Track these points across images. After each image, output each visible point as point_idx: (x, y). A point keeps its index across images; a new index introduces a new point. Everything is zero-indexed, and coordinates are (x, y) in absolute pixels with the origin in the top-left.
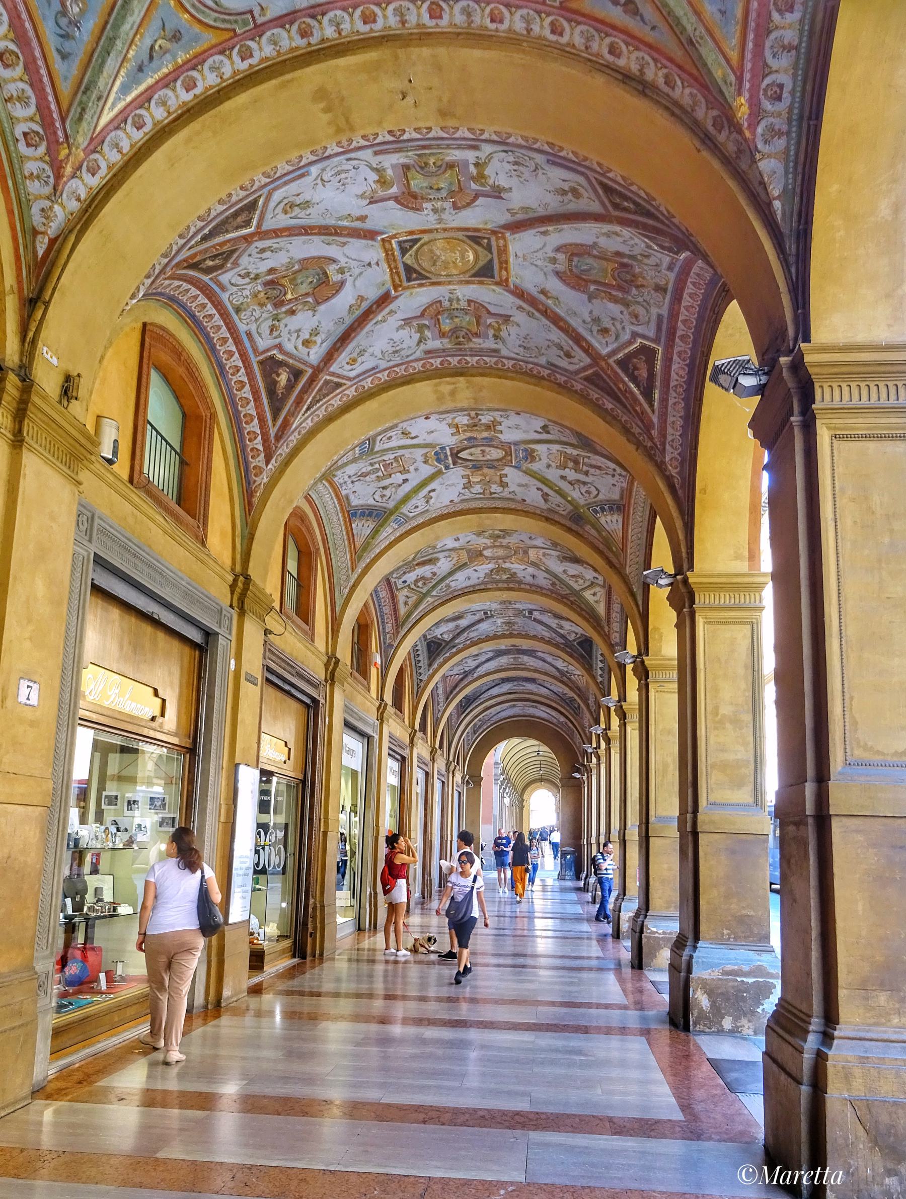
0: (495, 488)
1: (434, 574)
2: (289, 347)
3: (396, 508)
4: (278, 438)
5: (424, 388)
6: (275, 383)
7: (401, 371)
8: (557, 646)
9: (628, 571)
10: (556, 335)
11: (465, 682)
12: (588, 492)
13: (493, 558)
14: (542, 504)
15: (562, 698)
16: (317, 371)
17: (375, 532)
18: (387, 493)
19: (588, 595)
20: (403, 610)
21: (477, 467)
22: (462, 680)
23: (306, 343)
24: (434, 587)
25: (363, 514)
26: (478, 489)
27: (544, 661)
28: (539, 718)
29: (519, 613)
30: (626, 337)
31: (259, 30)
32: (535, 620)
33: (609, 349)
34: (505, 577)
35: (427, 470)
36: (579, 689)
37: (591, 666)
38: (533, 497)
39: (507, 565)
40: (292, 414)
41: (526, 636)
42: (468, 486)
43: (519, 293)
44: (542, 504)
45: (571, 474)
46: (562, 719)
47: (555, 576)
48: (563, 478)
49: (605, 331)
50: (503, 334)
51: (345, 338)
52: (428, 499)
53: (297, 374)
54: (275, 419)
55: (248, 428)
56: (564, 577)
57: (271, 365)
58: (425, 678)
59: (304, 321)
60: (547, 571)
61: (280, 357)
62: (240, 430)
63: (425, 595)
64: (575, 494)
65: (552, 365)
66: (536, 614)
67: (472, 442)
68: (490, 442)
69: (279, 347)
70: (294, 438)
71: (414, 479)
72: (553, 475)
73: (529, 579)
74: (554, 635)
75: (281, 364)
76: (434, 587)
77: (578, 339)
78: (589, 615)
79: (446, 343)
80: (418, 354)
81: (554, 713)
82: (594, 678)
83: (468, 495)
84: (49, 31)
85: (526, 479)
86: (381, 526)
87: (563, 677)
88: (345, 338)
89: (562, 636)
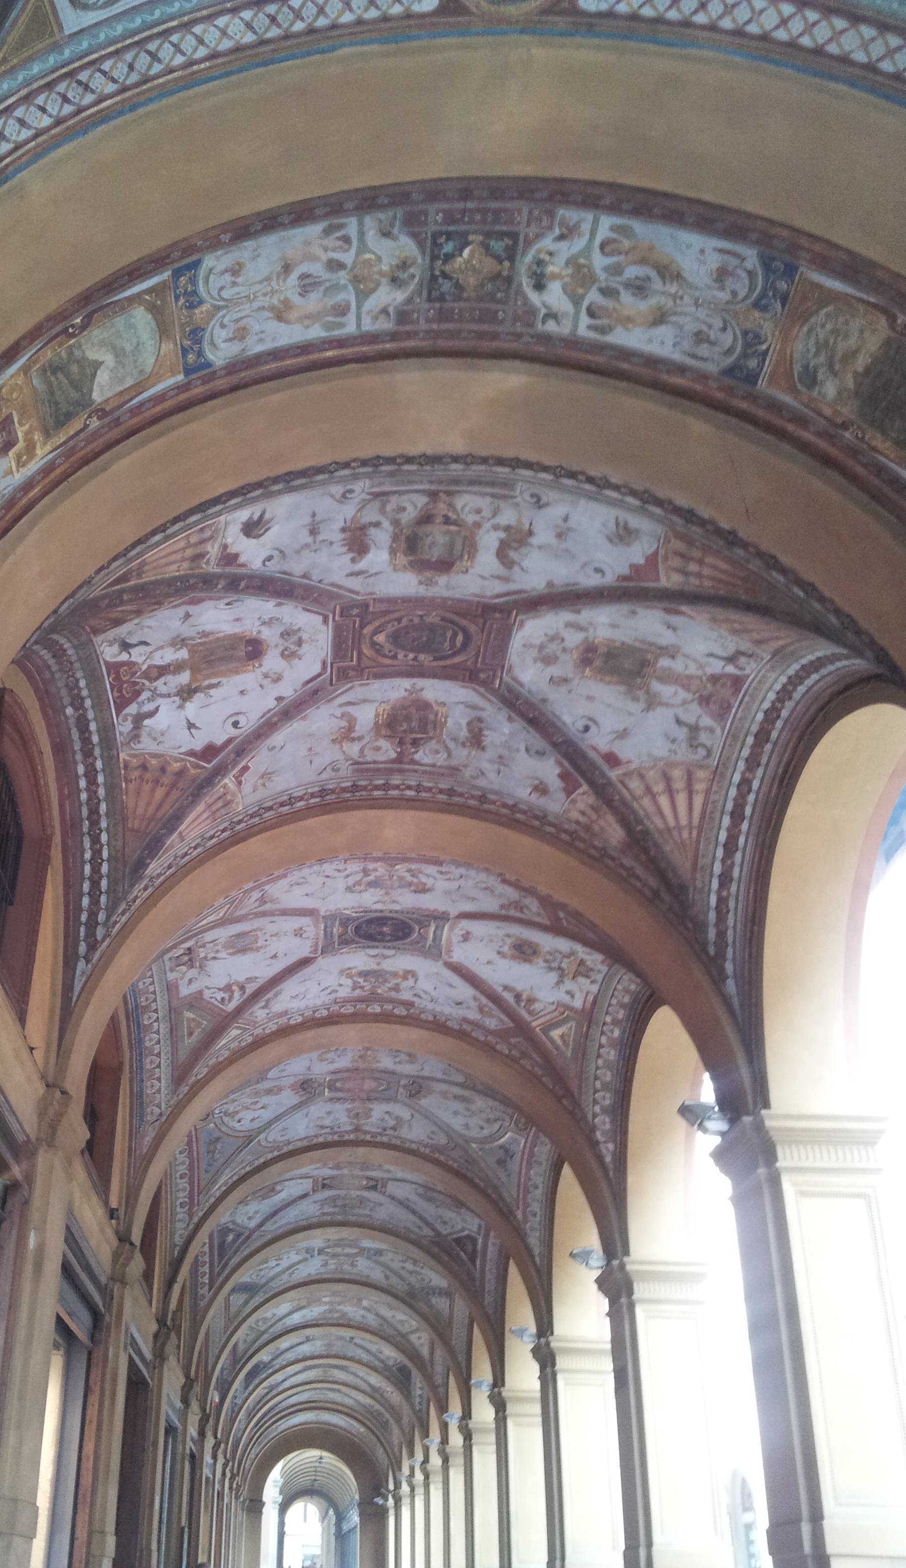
0: (345, 1267)
1: (274, 1315)
2: (239, 1221)
3: (267, 1283)
4: (219, 1274)
5: (317, 1232)
6: (224, 1242)
7: (304, 1223)
8: (375, 1369)
9: (453, 1343)
10: (411, 1217)
11: (269, 1396)
12: (423, 1279)
13: (329, 1302)
14: (383, 1280)
15: (368, 1410)
16: (252, 1232)
17: (246, 1302)
18: (262, 1273)
19: (413, 1338)
20: (241, 1347)
21: (334, 1256)
22: (267, 1393)
23: (250, 1218)
24: (272, 1326)
25: (240, 1289)
26: (333, 1267)
27: (357, 1376)
28: (336, 1426)
29: (341, 1338)
30: (459, 1227)
31: (289, 1143)
32: (356, 1344)
33: (448, 1231)
34: (336, 1315)
35: (295, 1258)
36: (393, 1408)
37: (409, 1392)
38: (377, 1275)
39: (341, 1307)
40: (230, 1259)
41: (344, 1358)
42: (326, 1264)
43: (393, 1198)
44: (383, 1280)
45: (409, 1266)
46: (362, 1430)
47: (383, 1318)
48: (403, 1268)
49: (445, 1223)
50: (377, 1209)
51: (275, 1214)
52: (293, 1273)
53: (239, 1235)
54: (219, 1263)
55: (201, 1270)
56: (390, 1320)
57: (224, 1231)
58: (239, 1401)
59: (252, 1208)
60: (377, 1315)
61: (232, 1227)
62: (197, 1271)
63: (264, 1333)
64: (412, 1280)
65: (408, 1229)
66: (356, 1340)
67: (336, 1245)
68: (350, 1246)
69: (233, 1222)
70: (227, 1271)
71: (284, 1264)
72: (396, 1265)
73: (358, 1318)
74: (372, 1359)
75: (231, 1230)
76: (272, 1326)
77: (427, 1224)
78: (412, 1354)
79: (337, 1210)
80: (318, 1213)
81: (355, 1423)
82: (412, 1405)
83: (323, 1270)
84: (203, 1165)
85: (373, 1265)
86: (252, 1297)
87: (374, 1393)
88: (275, 1214)
89: (382, 1361)
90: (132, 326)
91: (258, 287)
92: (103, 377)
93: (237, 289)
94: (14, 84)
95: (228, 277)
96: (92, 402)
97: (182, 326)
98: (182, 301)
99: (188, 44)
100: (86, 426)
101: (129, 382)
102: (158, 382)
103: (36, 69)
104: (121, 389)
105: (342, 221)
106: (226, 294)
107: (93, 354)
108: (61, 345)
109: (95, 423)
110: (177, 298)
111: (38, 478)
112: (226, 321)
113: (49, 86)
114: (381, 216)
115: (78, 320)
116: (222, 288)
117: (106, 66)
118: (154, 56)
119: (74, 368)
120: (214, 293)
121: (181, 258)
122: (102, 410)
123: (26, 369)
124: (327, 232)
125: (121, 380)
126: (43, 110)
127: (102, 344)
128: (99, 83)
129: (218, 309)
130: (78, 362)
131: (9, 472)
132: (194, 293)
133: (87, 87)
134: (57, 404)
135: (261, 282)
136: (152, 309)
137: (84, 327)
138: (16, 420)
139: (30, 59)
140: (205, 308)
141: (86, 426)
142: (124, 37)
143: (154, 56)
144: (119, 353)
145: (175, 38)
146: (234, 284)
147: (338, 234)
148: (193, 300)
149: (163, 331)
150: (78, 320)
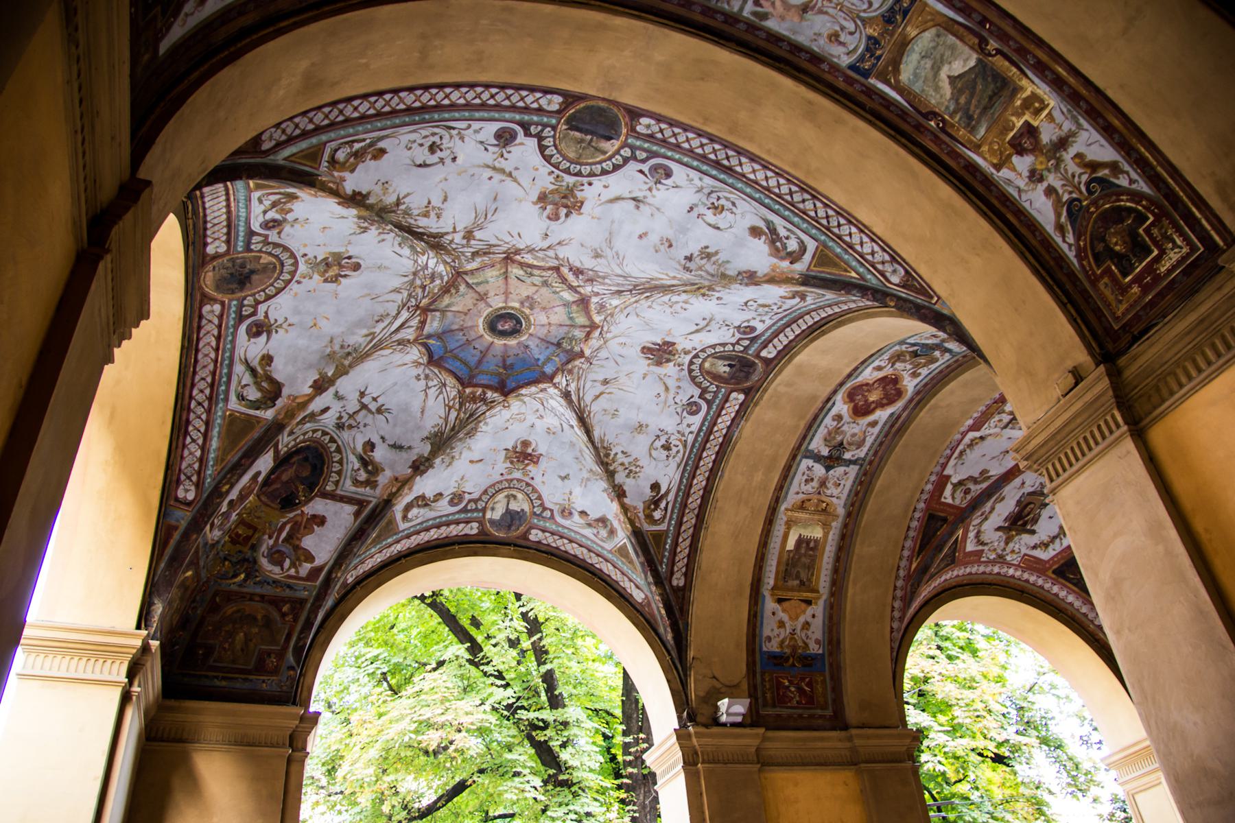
90: (916, 75)
91: (831, 11)
92: (958, 67)
93: (845, 23)
94: (851, 259)
95: (842, 39)
96: (979, 61)
97: (892, 35)
98: (879, 52)
99: (773, 183)
100: (999, 52)
101: (951, 39)
102: (939, 13)
103: (839, 250)
104: (958, 42)
105: (752, 18)
106: (851, 27)
107: (947, 90)
108: (953, 126)
109: (993, 44)
110: (880, 56)
111: (1050, 76)
112: (865, 6)
113: (840, 237)
114: (726, 7)
115: (932, 123)
116: (851, 34)
117: (812, 214)
118: (791, 193)
119: (962, 100)
120: (857, 35)
121: (857, 81)
122: (980, 45)
123: (976, 148)
124: (764, 16)
125: (953, 48)
126: (850, 234)
127: (937, 89)
128: (821, 213)
129: (863, 20)
130: (957, 103)
131: (1050, 117)
132: (867, 49)
133: (827, 217)
134: (991, 98)
135: (826, 13)
136: (897, 71)
137: (933, 115)
138: (1012, 134)
139: (837, 256)
140: (870, 31)
141: (999, 52)
142: (797, 215)
143: (791, 193)
144: (936, 69)
145: (777, 190)
146: (843, 28)
147: (759, 9)
148: (873, 42)
149: (903, 45)
150: (932, 123)
